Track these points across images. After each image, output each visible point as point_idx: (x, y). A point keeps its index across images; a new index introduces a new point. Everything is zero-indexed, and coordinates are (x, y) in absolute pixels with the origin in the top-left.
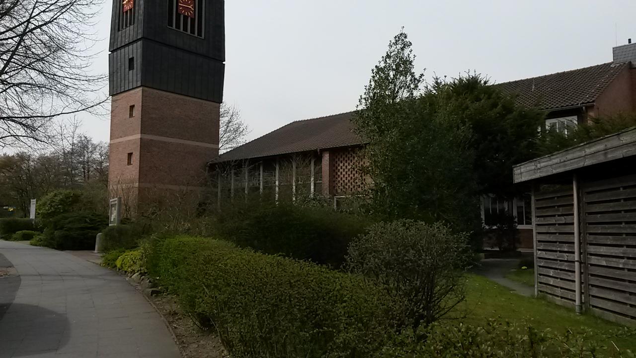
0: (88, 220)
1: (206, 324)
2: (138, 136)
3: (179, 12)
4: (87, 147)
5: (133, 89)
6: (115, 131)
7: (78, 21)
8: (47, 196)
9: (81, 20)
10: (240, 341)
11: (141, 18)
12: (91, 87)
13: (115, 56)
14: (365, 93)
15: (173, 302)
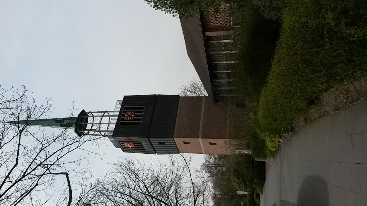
0: (248, 165)
1: (313, 101)
2: (200, 140)
3: (132, 119)
4: (207, 165)
5: (175, 142)
6: (198, 151)
7: (143, 170)
8: (235, 186)
9: (142, 169)
10: (328, 83)
11: (137, 138)
12: (176, 164)
13: (158, 151)
14: (170, 13)
15: (298, 120)
